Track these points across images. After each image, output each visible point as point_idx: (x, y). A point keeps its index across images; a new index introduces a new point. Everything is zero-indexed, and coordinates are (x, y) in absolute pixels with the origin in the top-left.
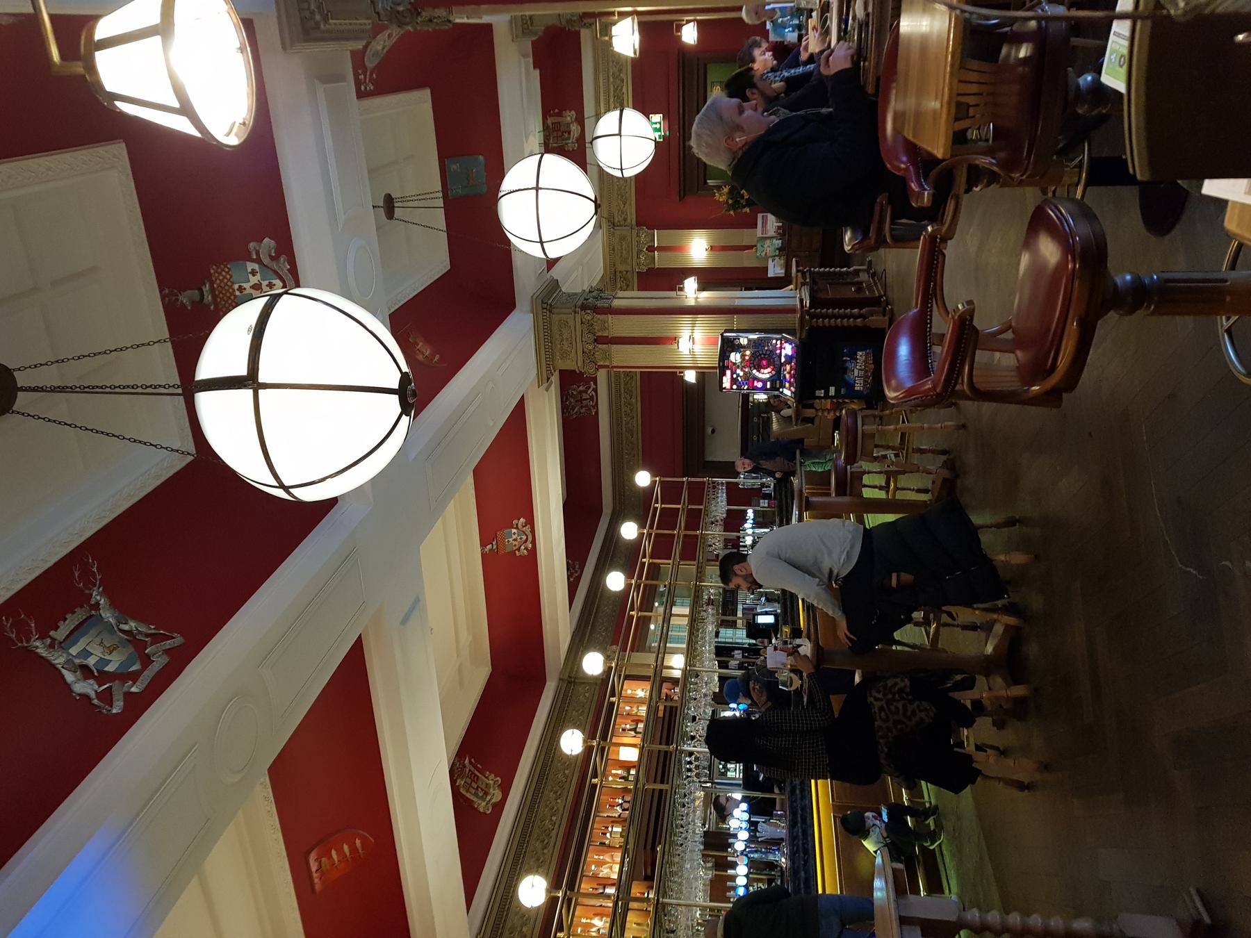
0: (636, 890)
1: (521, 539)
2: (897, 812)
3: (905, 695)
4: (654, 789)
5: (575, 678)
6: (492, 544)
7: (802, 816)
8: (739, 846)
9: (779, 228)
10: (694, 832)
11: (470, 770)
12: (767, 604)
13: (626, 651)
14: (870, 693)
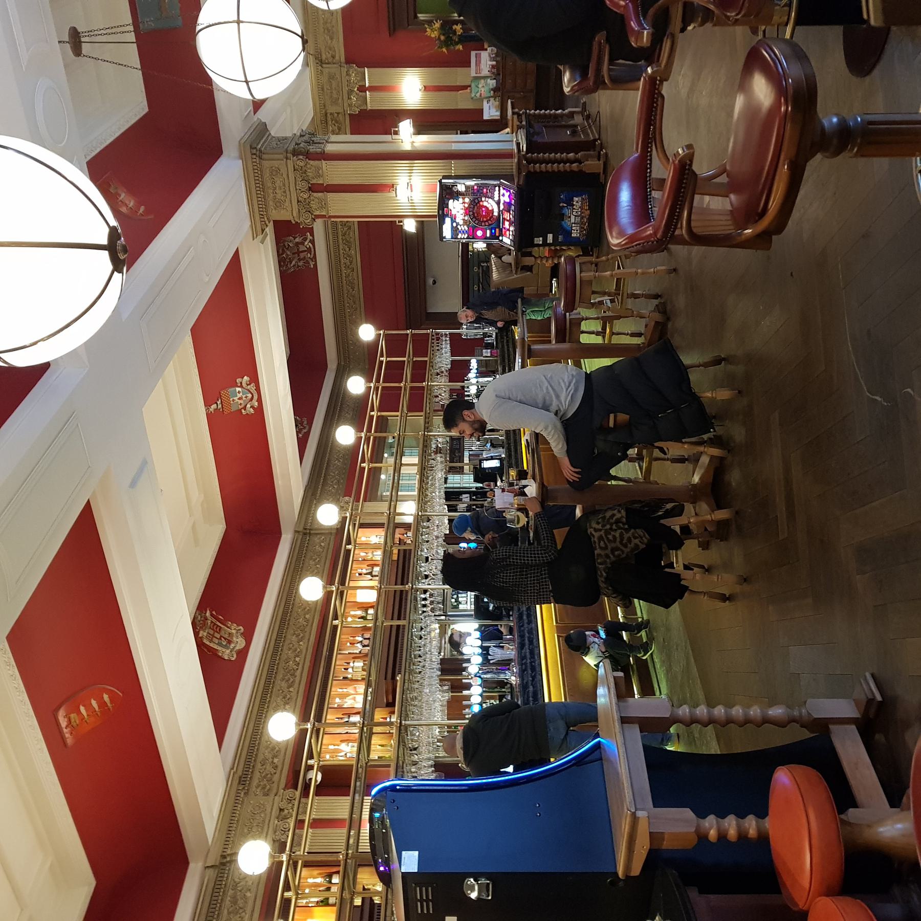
0: (379, 715)
1: (246, 397)
2: (613, 629)
3: (621, 525)
4: (391, 626)
5: (310, 530)
6: (217, 403)
7: (529, 638)
8: (473, 668)
9: (493, 67)
10: (431, 660)
11: (212, 622)
12: (492, 449)
13: (359, 502)
14: (590, 525)
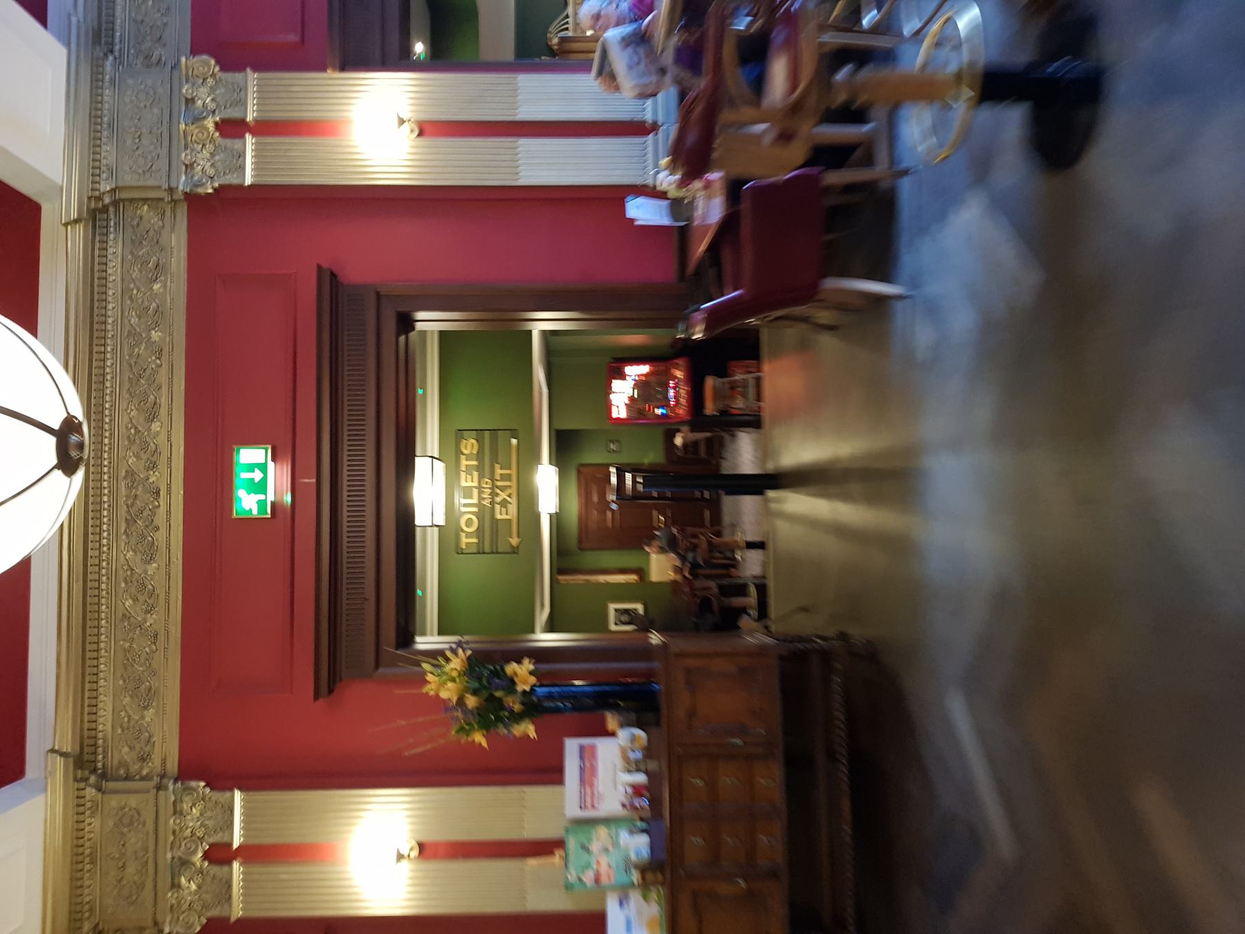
9: (637, 790)
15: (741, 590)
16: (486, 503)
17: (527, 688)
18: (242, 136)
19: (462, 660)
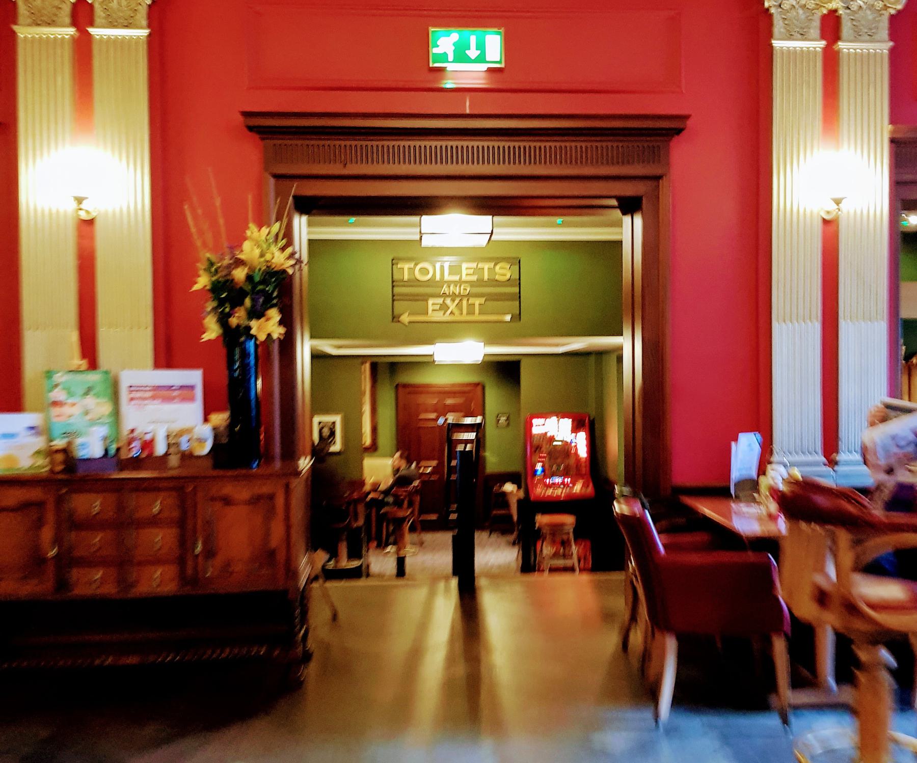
9: (148, 445)
15: (355, 554)
16: (445, 289)
17: (253, 332)
18: (823, 37)
19: (283, 264)
